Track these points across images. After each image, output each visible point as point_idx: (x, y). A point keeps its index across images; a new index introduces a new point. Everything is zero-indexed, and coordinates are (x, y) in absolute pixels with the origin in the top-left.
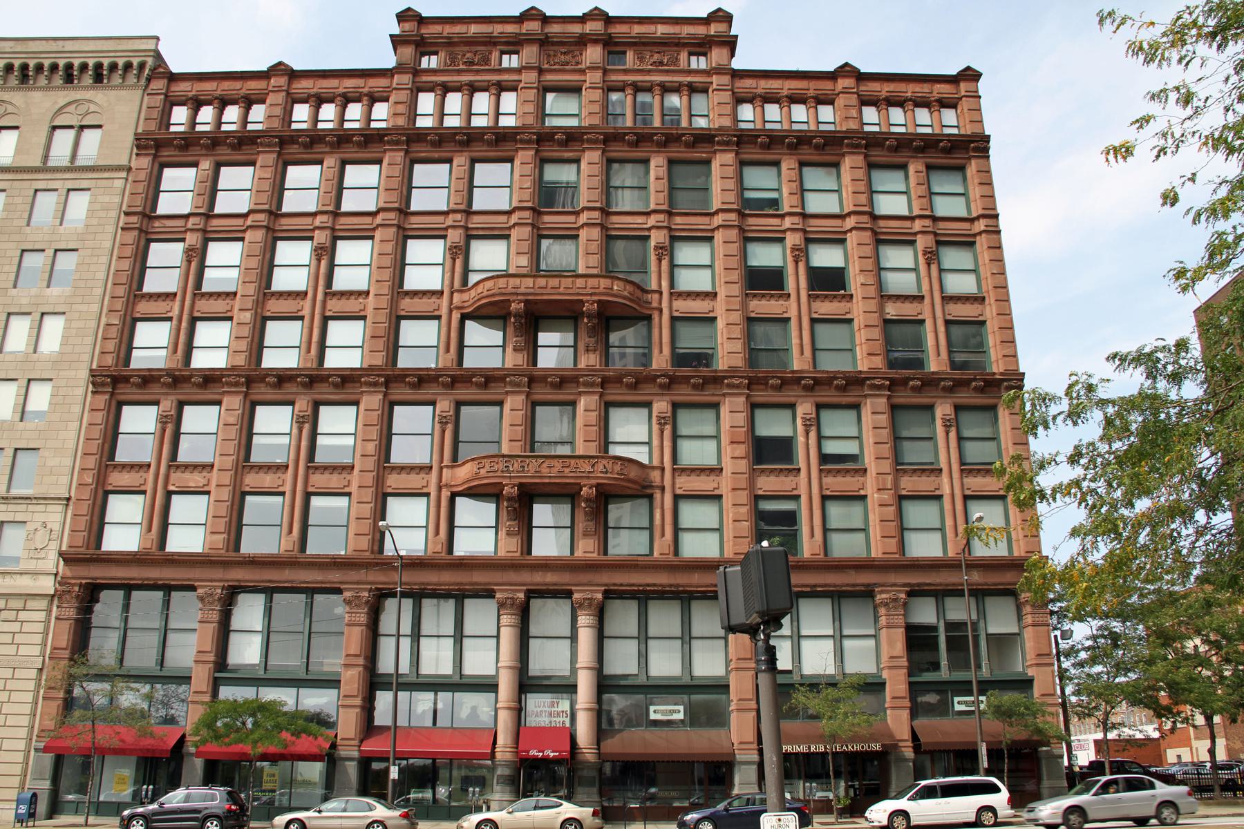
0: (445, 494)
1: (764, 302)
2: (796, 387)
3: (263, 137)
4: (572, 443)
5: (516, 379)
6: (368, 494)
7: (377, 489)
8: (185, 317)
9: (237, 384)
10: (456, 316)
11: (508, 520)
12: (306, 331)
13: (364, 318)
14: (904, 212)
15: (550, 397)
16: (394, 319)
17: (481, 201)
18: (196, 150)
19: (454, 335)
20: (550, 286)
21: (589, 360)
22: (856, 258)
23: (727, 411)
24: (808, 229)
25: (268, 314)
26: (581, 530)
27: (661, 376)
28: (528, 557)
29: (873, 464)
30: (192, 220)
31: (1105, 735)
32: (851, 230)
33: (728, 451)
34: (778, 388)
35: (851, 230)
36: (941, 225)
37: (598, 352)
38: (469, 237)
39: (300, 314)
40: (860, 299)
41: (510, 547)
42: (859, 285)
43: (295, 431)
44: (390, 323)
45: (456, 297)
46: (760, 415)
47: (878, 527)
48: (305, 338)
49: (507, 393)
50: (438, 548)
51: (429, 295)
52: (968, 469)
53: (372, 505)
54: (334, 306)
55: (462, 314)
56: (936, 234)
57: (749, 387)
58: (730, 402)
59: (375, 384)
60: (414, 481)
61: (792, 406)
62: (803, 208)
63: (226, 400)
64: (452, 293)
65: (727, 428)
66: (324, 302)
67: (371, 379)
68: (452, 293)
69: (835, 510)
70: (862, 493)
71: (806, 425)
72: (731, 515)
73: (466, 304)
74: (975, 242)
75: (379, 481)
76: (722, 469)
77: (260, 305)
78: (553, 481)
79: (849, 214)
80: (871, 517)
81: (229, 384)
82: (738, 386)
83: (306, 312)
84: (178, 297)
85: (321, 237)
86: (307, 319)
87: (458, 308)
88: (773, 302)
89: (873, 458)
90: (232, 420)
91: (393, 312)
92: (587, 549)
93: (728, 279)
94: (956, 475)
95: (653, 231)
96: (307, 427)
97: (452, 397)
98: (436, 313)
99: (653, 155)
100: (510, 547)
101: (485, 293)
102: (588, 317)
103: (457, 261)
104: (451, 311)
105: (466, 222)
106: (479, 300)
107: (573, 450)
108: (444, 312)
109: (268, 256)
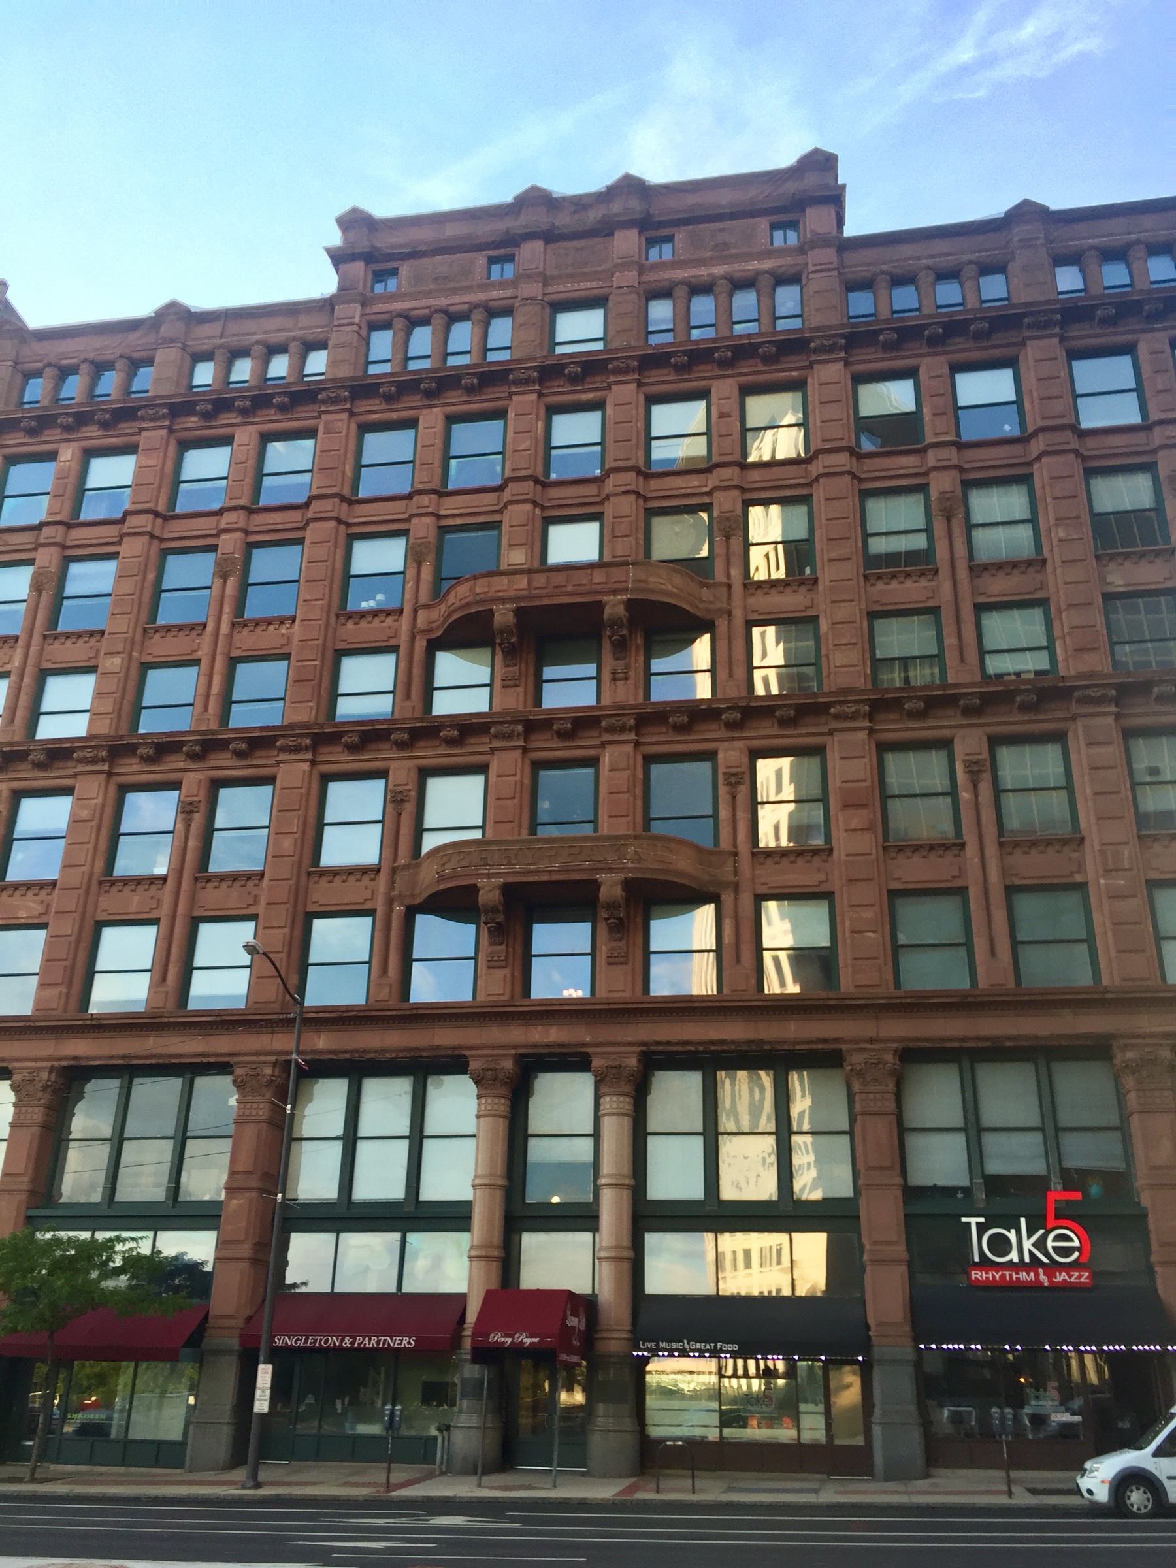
0: (399, 909)
1: (894, 585)
2: (950, 712)
3: (146, 406)
4: (595, 822)
5: (505, 729)
6: (281, 916)
7: (295, 906)
8: (29, 670)
9: (94, 761)
10: (421, 644)
11: (491, 944)
12: (203, 680)
13: (286, 656)
14: (1135, 419)
15: (558, 754)
16: (329, 655)
17: (273, 490)
18: (55, 434)
19: (417, 671)
20: (493, 589)
21: (625, 694)
22: (1049, 500)
23: (837, 755)
24: (966, 466)
25: (149, 659)
26: (604, 956)
27: (728, 708)
28: (525, 1002)
29: (1094, 829)
30: (47, 532)
31: (93, 1235)
32: (1039, 458)
33: (841, 821)
34: (922, 715)
35: (1039, 458)
36: (970, 454)
37: (520, 689)
38: (67, 561)
39: (195, 656)
40: (1058, 563)
41: (498, 986)
42: (1055, 542)
43: (179, 826)
44: (322, 661)
45: (422, 615)
46: (892, 760)
47: (1110, 934)
48: (202, 689)
49: (492, 751)
50: (384, 994)
51: (382, 617)
52: (1008, 844)
53: (286, 931)
54: (246, 641)
55: (428, 641)
56: (961, 469)
57: (871, 716)
58: (839, 741)
59: (298, 749)
60: (353, 892)
61: (945, 744)
62: (958, 435)
63: (80, 785)
64: (415, 611)
65: (838, 784)
66: (230, 636)
67: (290, 742)
68: (415, 611)
69: (1027, 905)
70: (1078, 878)
71: (729, 784)
72: (848, 923)
73: (434, 625)
74: (1031, 475)
75: (298, 894)
76: (831, 850)
77: (137, 647)
78: (555, 877)
79: (1035, 434)
80: (1096, 917)
81: (82, 761)
82: (853, 717)
83: (203, 653)
84: (20, 643)
85: (230, 543)
86: (205, 663)
87: (423, 632)
88: (909, 583)
89: (1093, 819)
90: (85, 814)
91: (329, 644)
92: (617, 986)
93: (833, 555)
94: (991, 850)
95: (716, 494)
96: (198, 819)
97: (411, 763)
98: (392, 642)
99: (62, 445)
100: (498, 986)
101: (458, 604)
102: (611, 627)
103: (44, 594)
104: (413, 638)
105: (438, 505)
106: (450, 615)
107: (596, 830)
108: (403, 640)
109: (151, 576)
